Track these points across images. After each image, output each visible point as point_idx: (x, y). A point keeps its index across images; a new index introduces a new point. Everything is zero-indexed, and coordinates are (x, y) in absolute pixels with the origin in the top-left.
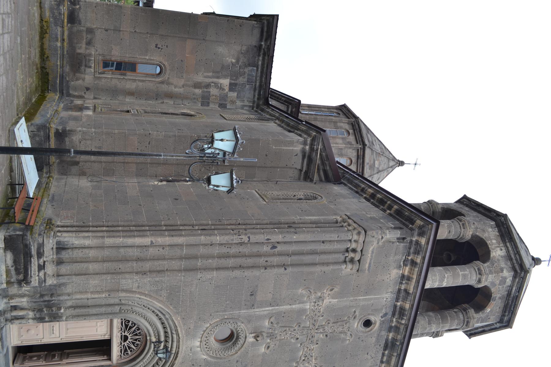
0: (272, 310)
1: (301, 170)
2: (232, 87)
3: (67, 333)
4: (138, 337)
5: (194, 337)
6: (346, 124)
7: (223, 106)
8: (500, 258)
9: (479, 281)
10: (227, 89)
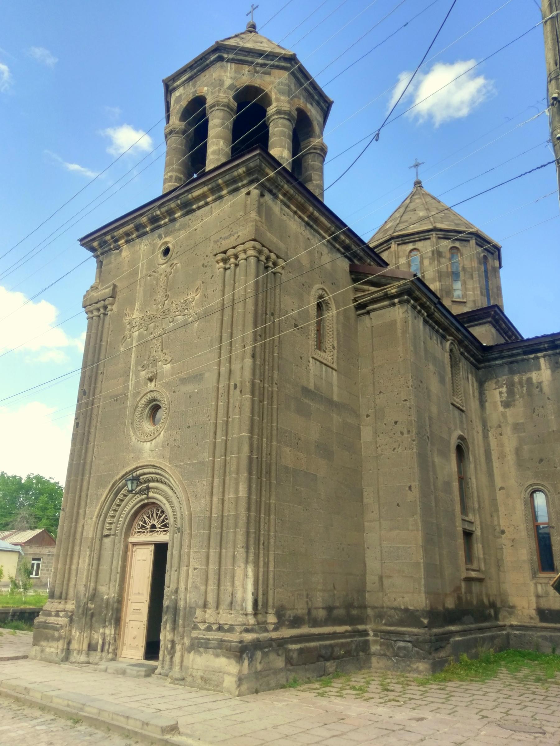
0: (132, 372)
3: (143, 594)
4: (155, 513)
5: (141, 451)
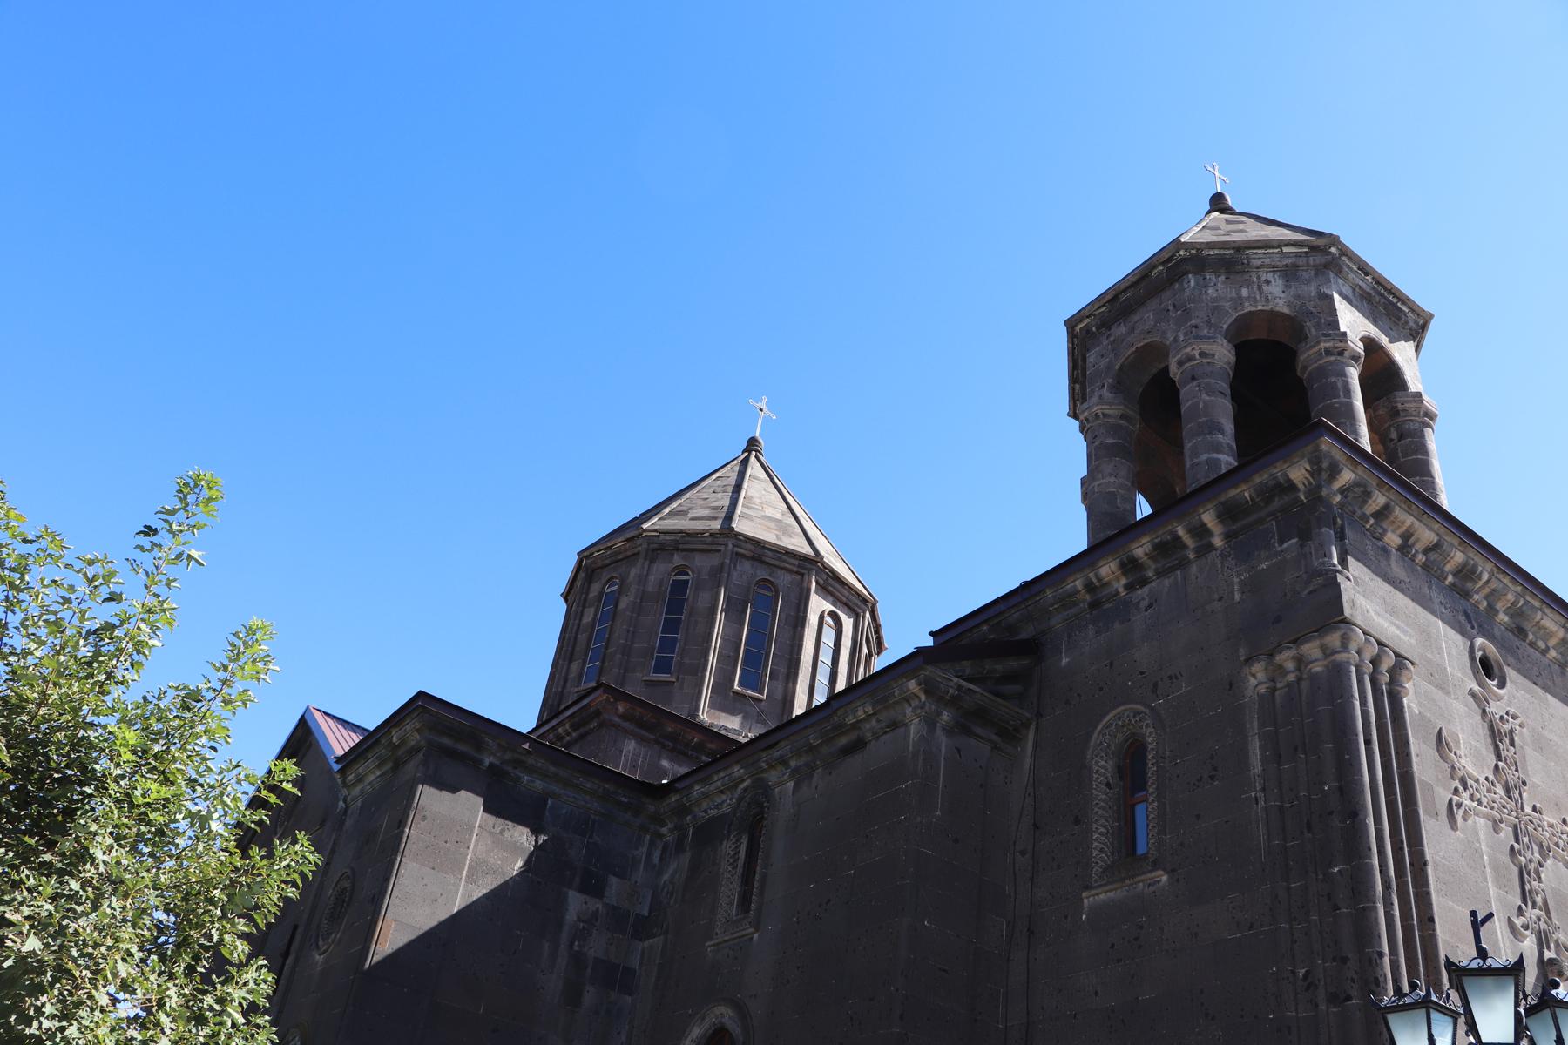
1: (995, 747)
2: (593, 887)
6: (655, 567)
7: (642, 928)
8: (1292, 291)
9: (1356, 358)
10: (596, 905)
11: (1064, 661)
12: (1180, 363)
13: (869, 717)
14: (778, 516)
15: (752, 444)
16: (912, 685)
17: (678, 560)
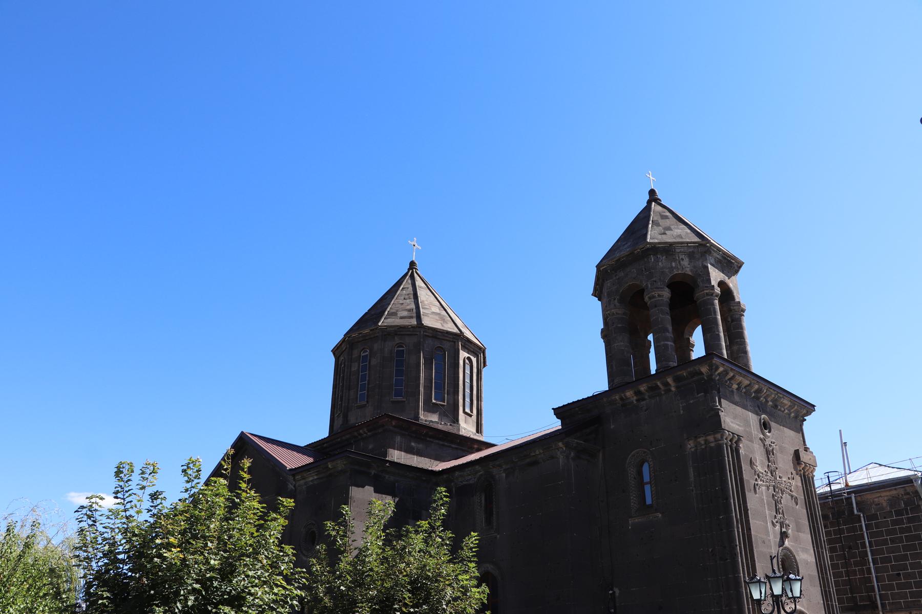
11: (612, 427)
12: (650, 298)
13: (540, 454)
14: (438, 311)
15: (412, 265)
16: (560, 444)
17: (397, 340)
